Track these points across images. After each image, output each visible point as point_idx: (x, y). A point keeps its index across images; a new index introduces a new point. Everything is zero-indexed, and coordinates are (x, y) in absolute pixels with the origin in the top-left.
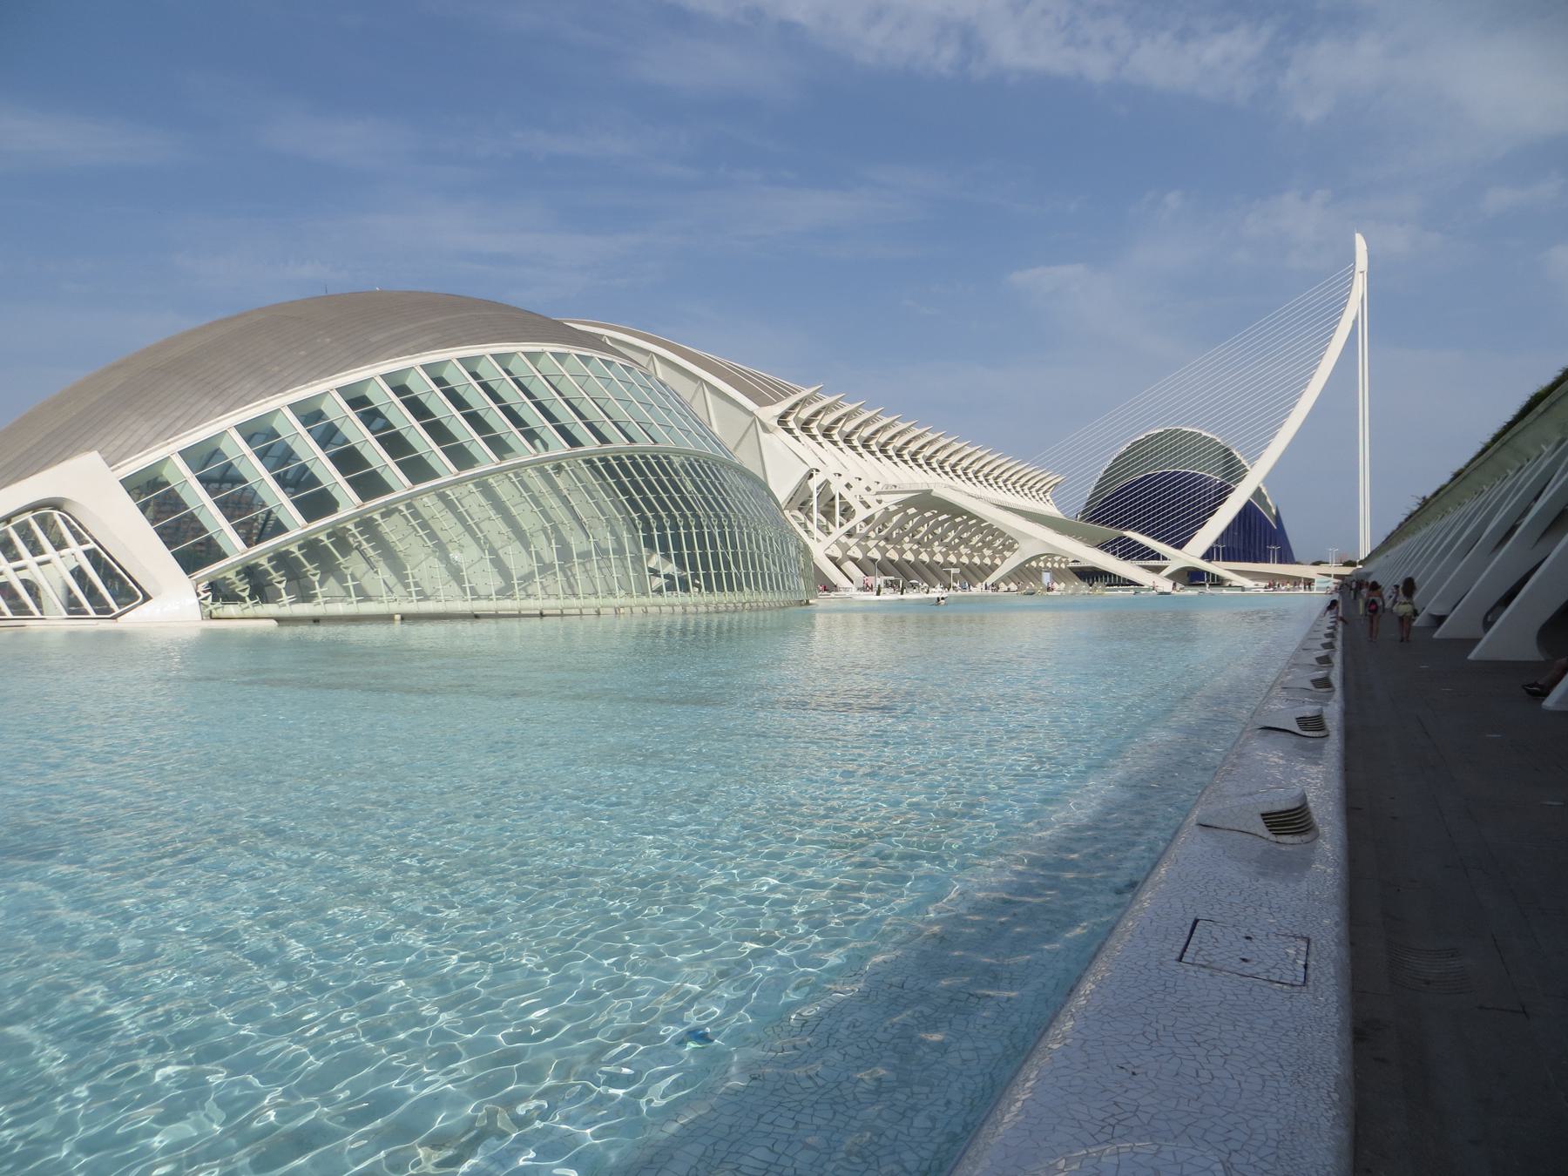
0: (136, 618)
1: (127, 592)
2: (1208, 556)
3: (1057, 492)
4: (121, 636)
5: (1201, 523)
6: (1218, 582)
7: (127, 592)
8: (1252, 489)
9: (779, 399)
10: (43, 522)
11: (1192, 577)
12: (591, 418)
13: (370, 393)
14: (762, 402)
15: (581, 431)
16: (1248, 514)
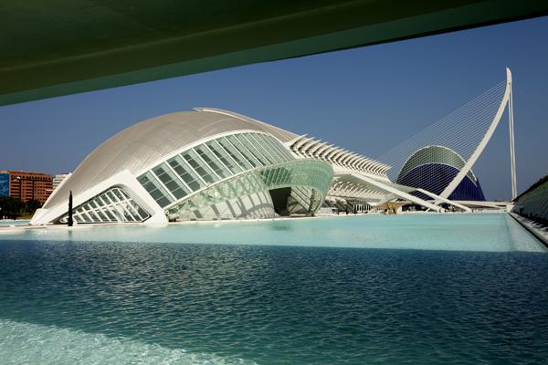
0: (401, 208)
1: (144, 215)
2: (450, 198)
3: (389, 174)
4: (144, 227)
5: (447, 185)
6: (455, 209)
7: (144, 215)
8: (467, 172)
9: (290, 140)
10: (116, 192)
11: (445, 206)
12: (243, 151)
13: (201, 149)
14: (285, 141)
15: (256, 161)
16: (466, 181)
